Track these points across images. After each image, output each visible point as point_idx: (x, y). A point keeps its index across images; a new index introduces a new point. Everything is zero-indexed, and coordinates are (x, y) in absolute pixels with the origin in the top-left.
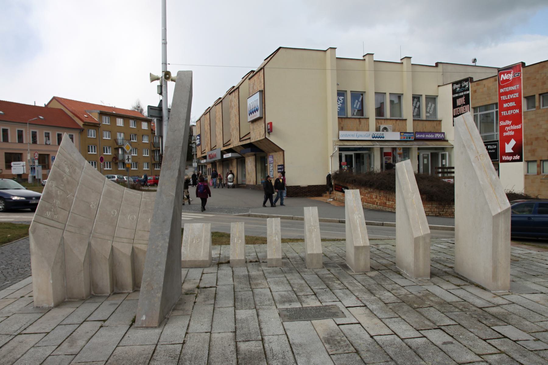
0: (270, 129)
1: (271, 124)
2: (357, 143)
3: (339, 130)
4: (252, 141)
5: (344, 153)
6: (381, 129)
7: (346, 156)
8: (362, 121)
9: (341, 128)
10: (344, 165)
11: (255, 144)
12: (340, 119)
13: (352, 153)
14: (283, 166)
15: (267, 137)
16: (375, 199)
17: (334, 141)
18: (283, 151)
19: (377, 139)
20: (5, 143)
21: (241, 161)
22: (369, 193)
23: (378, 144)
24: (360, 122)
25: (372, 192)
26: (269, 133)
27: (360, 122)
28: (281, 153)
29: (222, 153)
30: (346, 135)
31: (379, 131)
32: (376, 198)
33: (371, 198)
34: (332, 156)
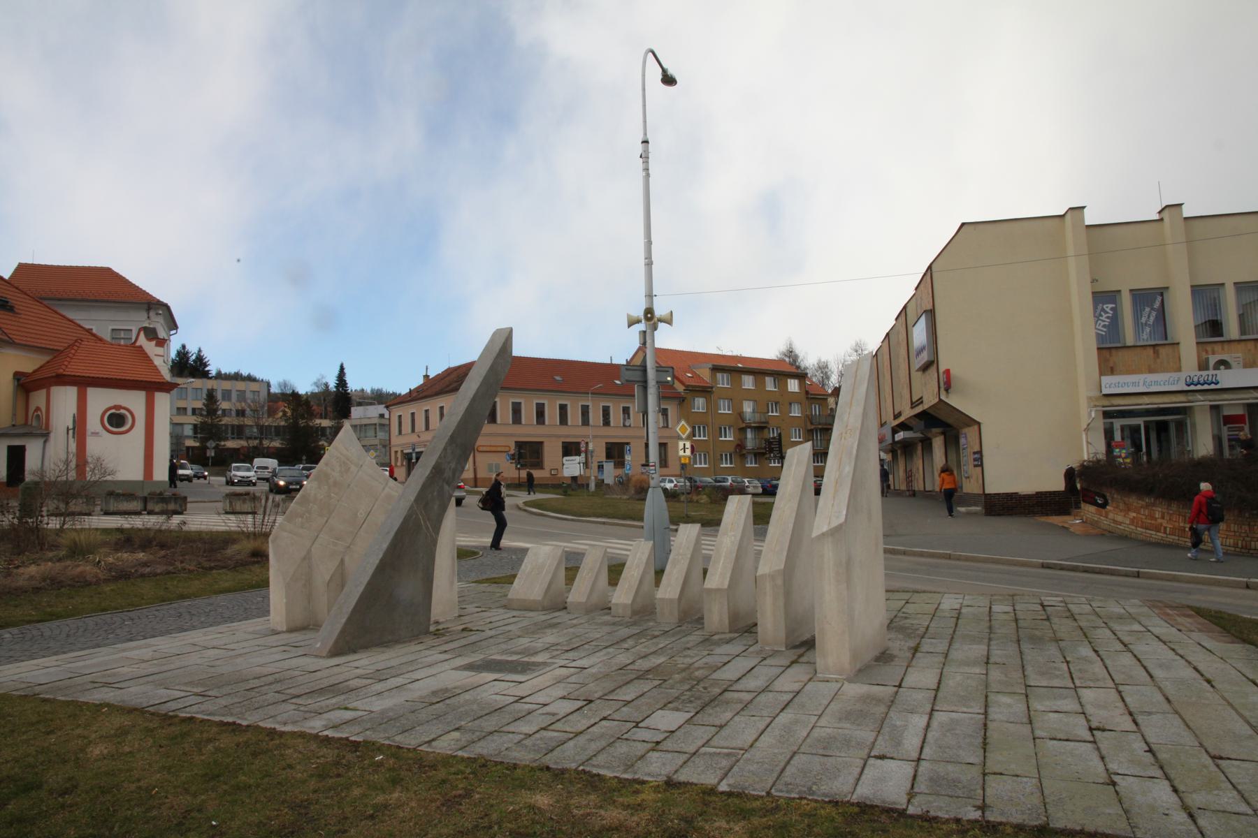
0: (947, 383)
1: (947, 372)
2: (1146, 399)
3: (1101, 374)
4: (926, 406)
5: (1118, 423)
6: (1212, 363)
7: (1123, 428)
8: (1162, 351)
9: (1107, 368)
10: (1117, 447)
11: (931, 412)
12: (1106, 353)
13: (1139, 421)
14: (980, 452)
15: (943, 397)
16: (1160, 521)
17: (1090, 399)
18: (979, 424)
19: (1199, 387)
20: (564, 427)
21: (927, 444)
22: (1147, 506)
23: (1200, 397)
24: (1156, 353)
25: (1154, 505)
26: (947, 390)
27: (1156, 353)
28: (976, 427)
29: (895, 431)
30: (1118, 385)
31: (1207, 368)
32: (1163, 518)
33: (1153, 518)
34: (1087, 430)
